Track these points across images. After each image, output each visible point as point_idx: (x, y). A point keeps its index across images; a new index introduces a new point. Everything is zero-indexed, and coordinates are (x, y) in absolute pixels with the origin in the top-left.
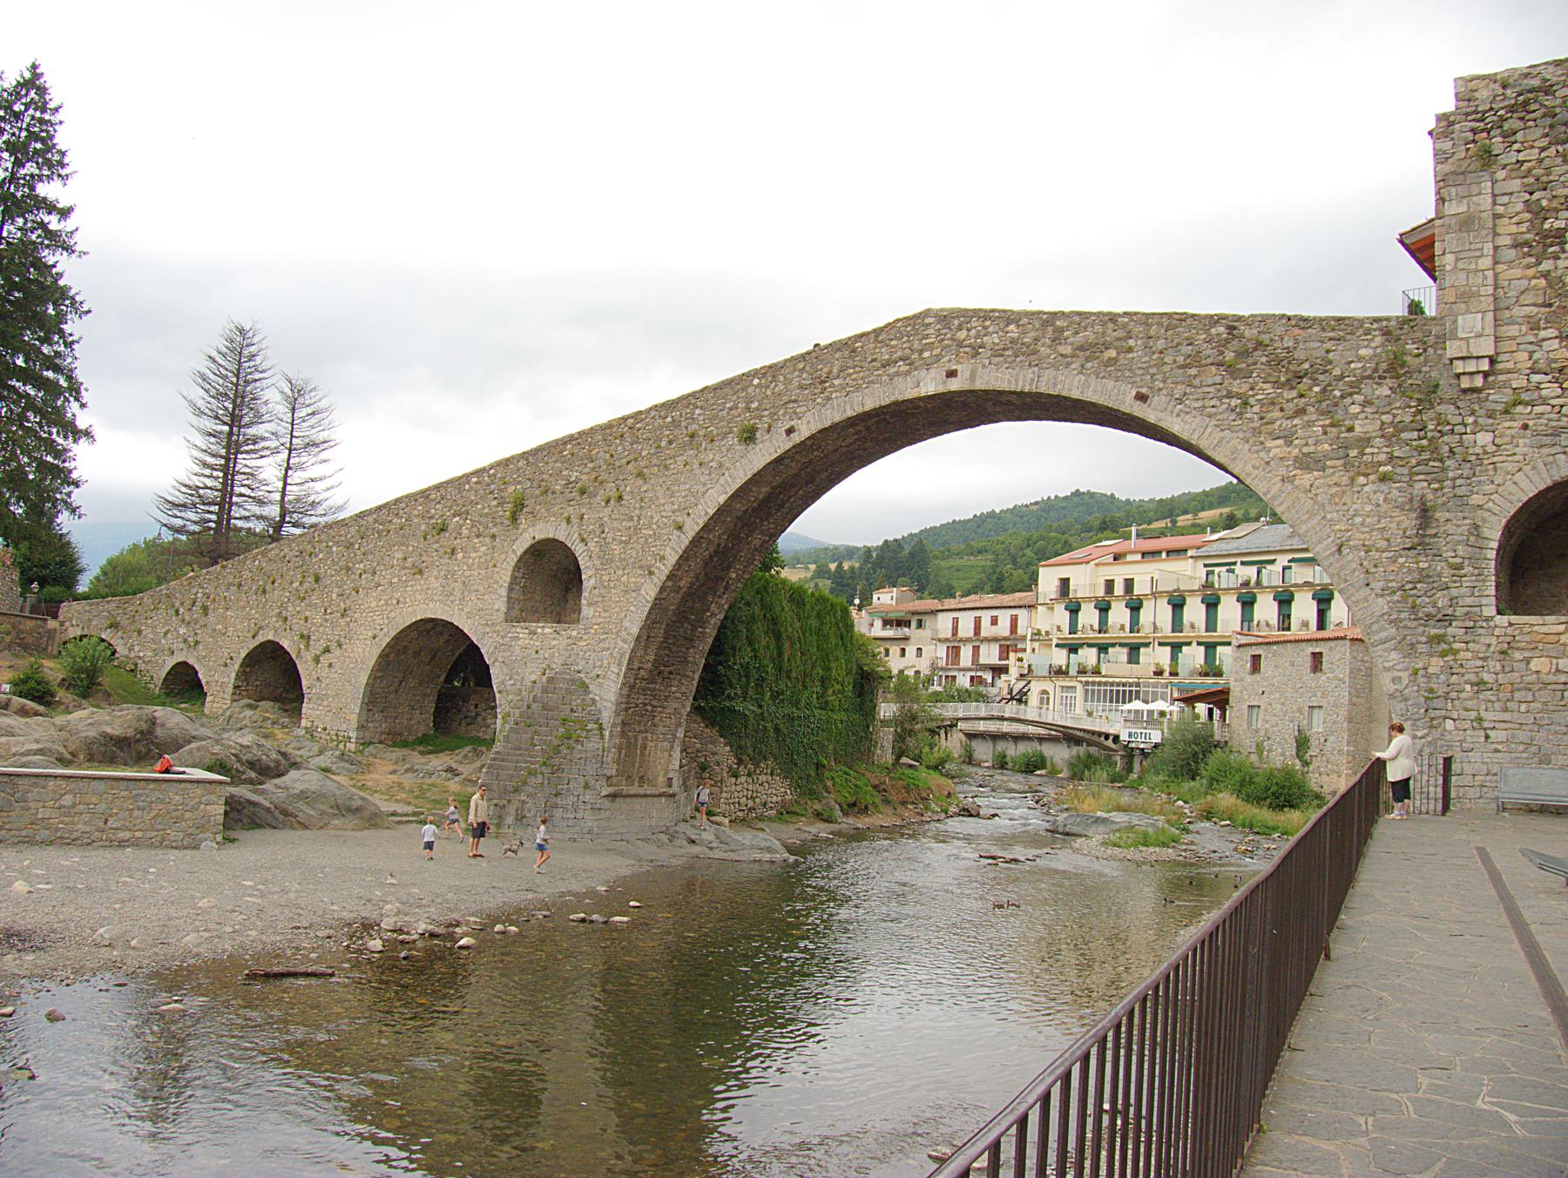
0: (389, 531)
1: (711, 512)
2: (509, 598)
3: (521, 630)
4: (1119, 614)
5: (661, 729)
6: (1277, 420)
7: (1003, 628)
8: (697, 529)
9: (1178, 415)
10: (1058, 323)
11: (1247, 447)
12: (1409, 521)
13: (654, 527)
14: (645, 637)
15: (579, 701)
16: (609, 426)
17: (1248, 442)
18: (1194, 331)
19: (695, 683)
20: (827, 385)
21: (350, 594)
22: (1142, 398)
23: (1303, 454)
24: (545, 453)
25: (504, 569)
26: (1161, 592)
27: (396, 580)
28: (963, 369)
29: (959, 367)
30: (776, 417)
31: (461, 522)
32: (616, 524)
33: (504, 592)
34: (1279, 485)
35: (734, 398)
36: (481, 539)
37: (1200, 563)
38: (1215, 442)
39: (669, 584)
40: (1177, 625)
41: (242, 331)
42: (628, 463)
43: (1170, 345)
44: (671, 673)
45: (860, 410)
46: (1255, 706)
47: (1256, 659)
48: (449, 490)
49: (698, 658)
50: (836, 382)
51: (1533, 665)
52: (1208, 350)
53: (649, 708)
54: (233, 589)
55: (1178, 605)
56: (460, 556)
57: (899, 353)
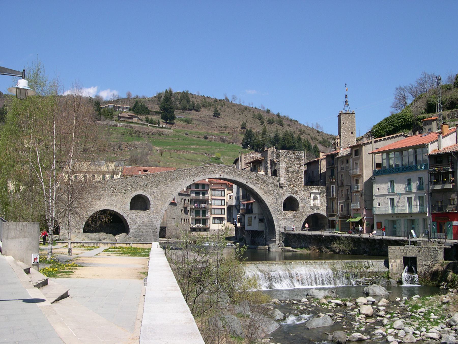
3: (134, 212)
12: (275, 200)
22: (247, 183)
51: (287, 216)
52: (254, 177)
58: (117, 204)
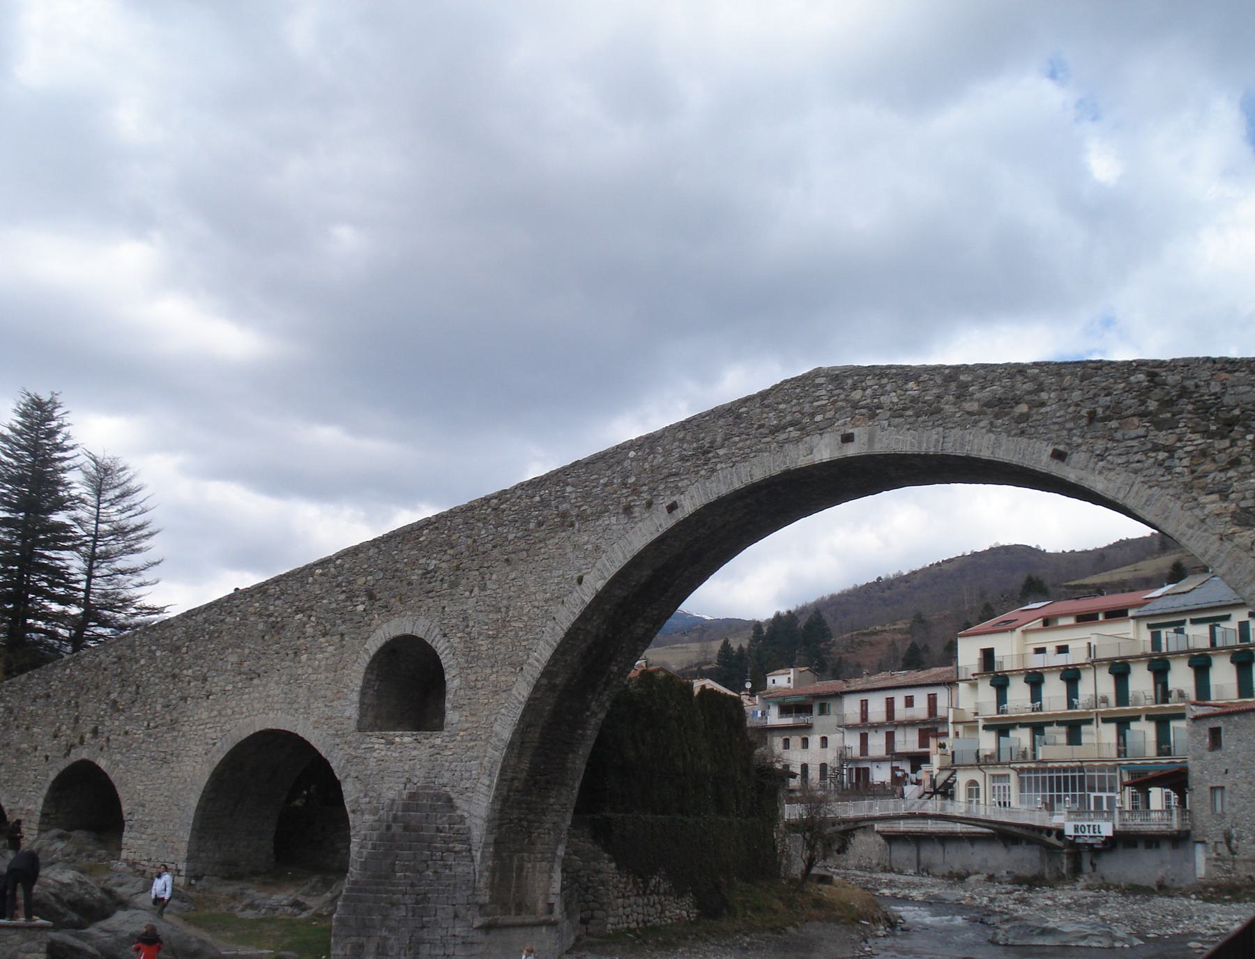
0: (221, 632)
1: (588, 600)
2: (362, 703)
3: (376, 741)
4: (1054, 693)
5: (539, 847)
6: (1210, 472)
7: (920, 709)
8: (573, 619)
9: (1100, 473)
10: (962, 378)
11: (1179, 504)
13: (525, 618)
14: (517, 744)
15: (445, 819)
16: (470, 508)
17: (1179, 498)
18: (1112, 380)
19: (576, 792)
20: (711, 455)
21: (177, 704)
22: (1059, 456)
23: (1242, 508)
24: (398, 539)
25: (354, 671)
26: (1100, 660)
27: (230, 687)
28: (860, 433)
29: (855, 431)
30: (655, 493)
31: (305, 619)
32: (481, 617)
33: (355, 697)
34: (1218, 543)
35: (608, 473)
36: (328, 638)
37: (1143, 626)
38: (1143, 500)
39: (544, 681)
40: (1122, 694)
41: (38, 404)
42: (494, 547)
43: (1087, 396)
44: (548, 782)
45: (747, 481)
46: (1218, 787)
47: (1215, 734)
48: (290, 583)
49: (578, 762)
50: (721, 452)
52: (1130, 401)
53: (525, 823)
54: (41, 701)
55: (1120, 671)
56: (304, 657)
57: (789, 418)
58: (312, 700)
